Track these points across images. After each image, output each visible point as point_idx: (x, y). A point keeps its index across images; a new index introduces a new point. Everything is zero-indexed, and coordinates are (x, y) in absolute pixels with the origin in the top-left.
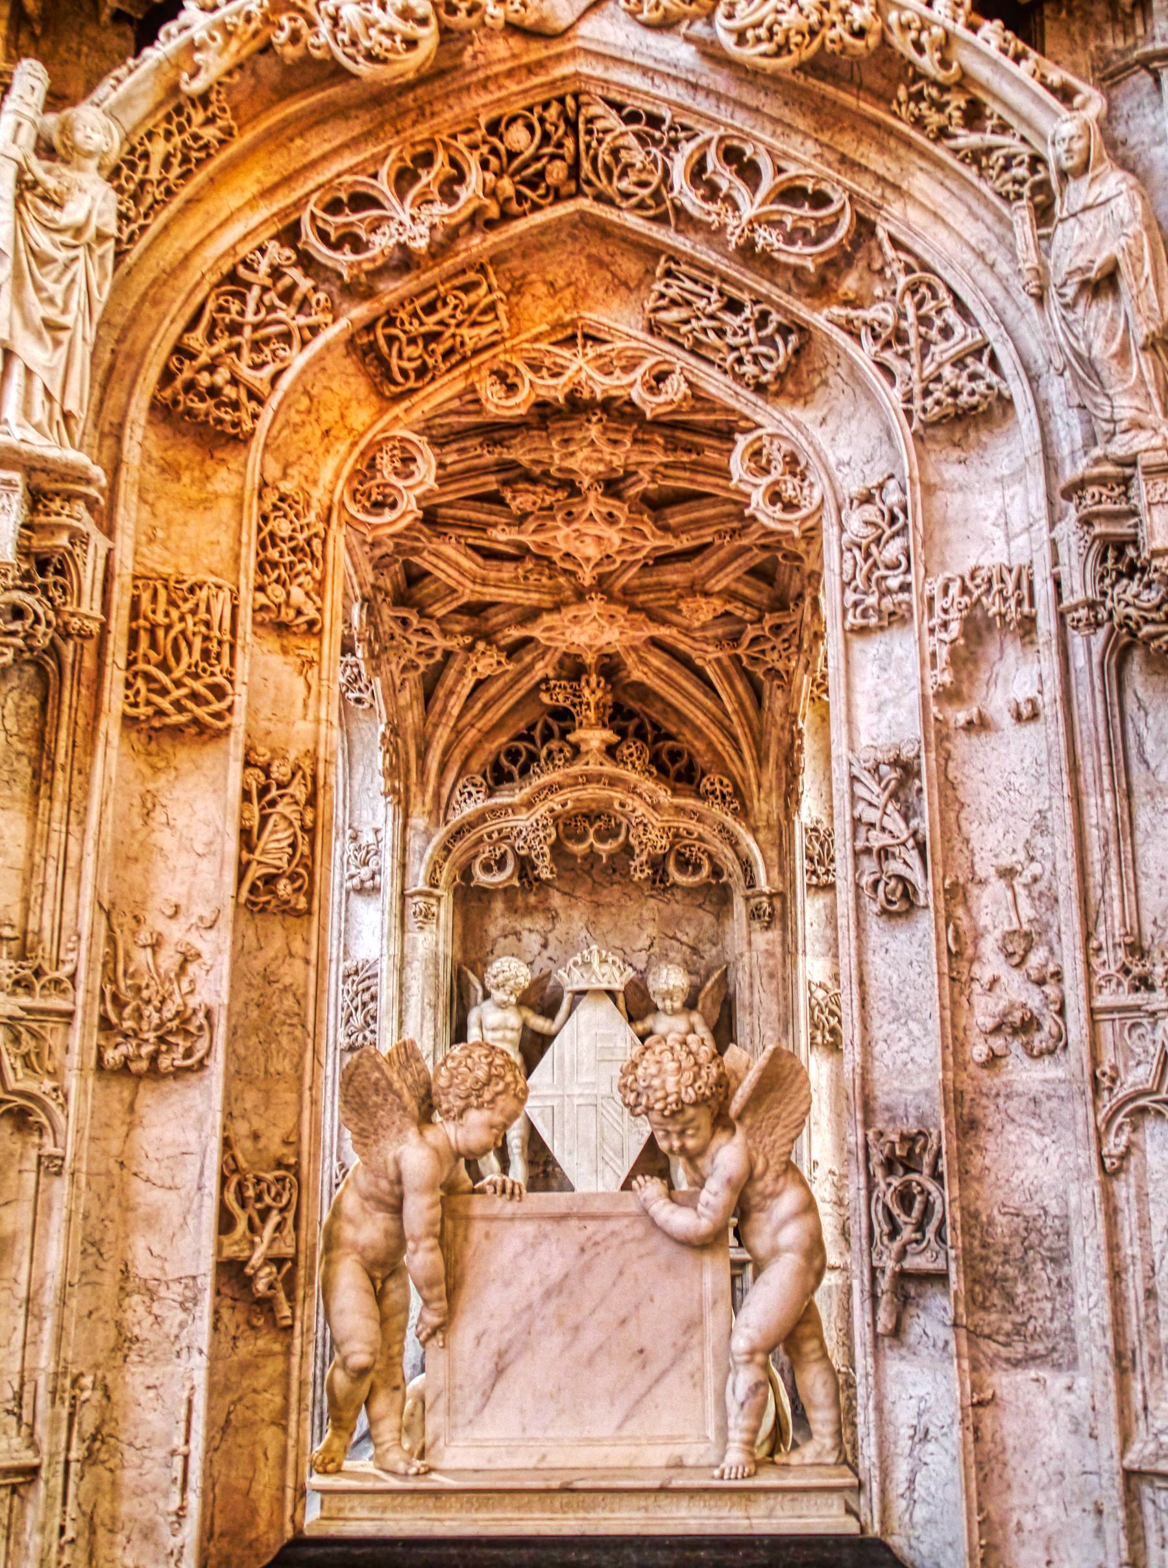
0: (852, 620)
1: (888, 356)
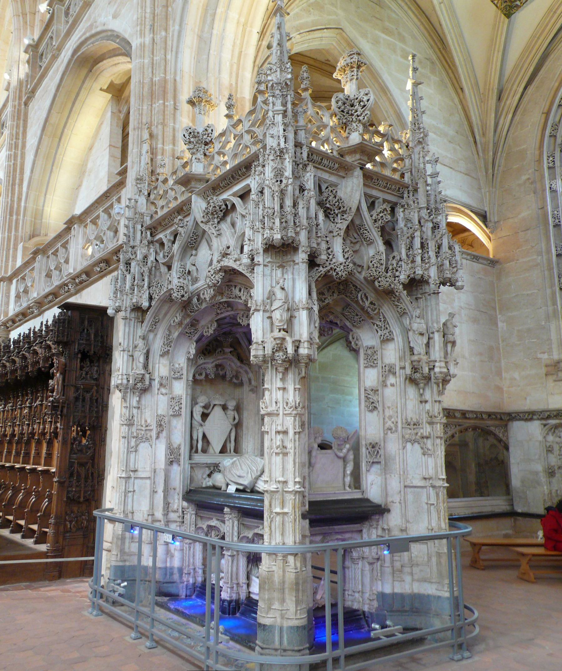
1: (378, 330)
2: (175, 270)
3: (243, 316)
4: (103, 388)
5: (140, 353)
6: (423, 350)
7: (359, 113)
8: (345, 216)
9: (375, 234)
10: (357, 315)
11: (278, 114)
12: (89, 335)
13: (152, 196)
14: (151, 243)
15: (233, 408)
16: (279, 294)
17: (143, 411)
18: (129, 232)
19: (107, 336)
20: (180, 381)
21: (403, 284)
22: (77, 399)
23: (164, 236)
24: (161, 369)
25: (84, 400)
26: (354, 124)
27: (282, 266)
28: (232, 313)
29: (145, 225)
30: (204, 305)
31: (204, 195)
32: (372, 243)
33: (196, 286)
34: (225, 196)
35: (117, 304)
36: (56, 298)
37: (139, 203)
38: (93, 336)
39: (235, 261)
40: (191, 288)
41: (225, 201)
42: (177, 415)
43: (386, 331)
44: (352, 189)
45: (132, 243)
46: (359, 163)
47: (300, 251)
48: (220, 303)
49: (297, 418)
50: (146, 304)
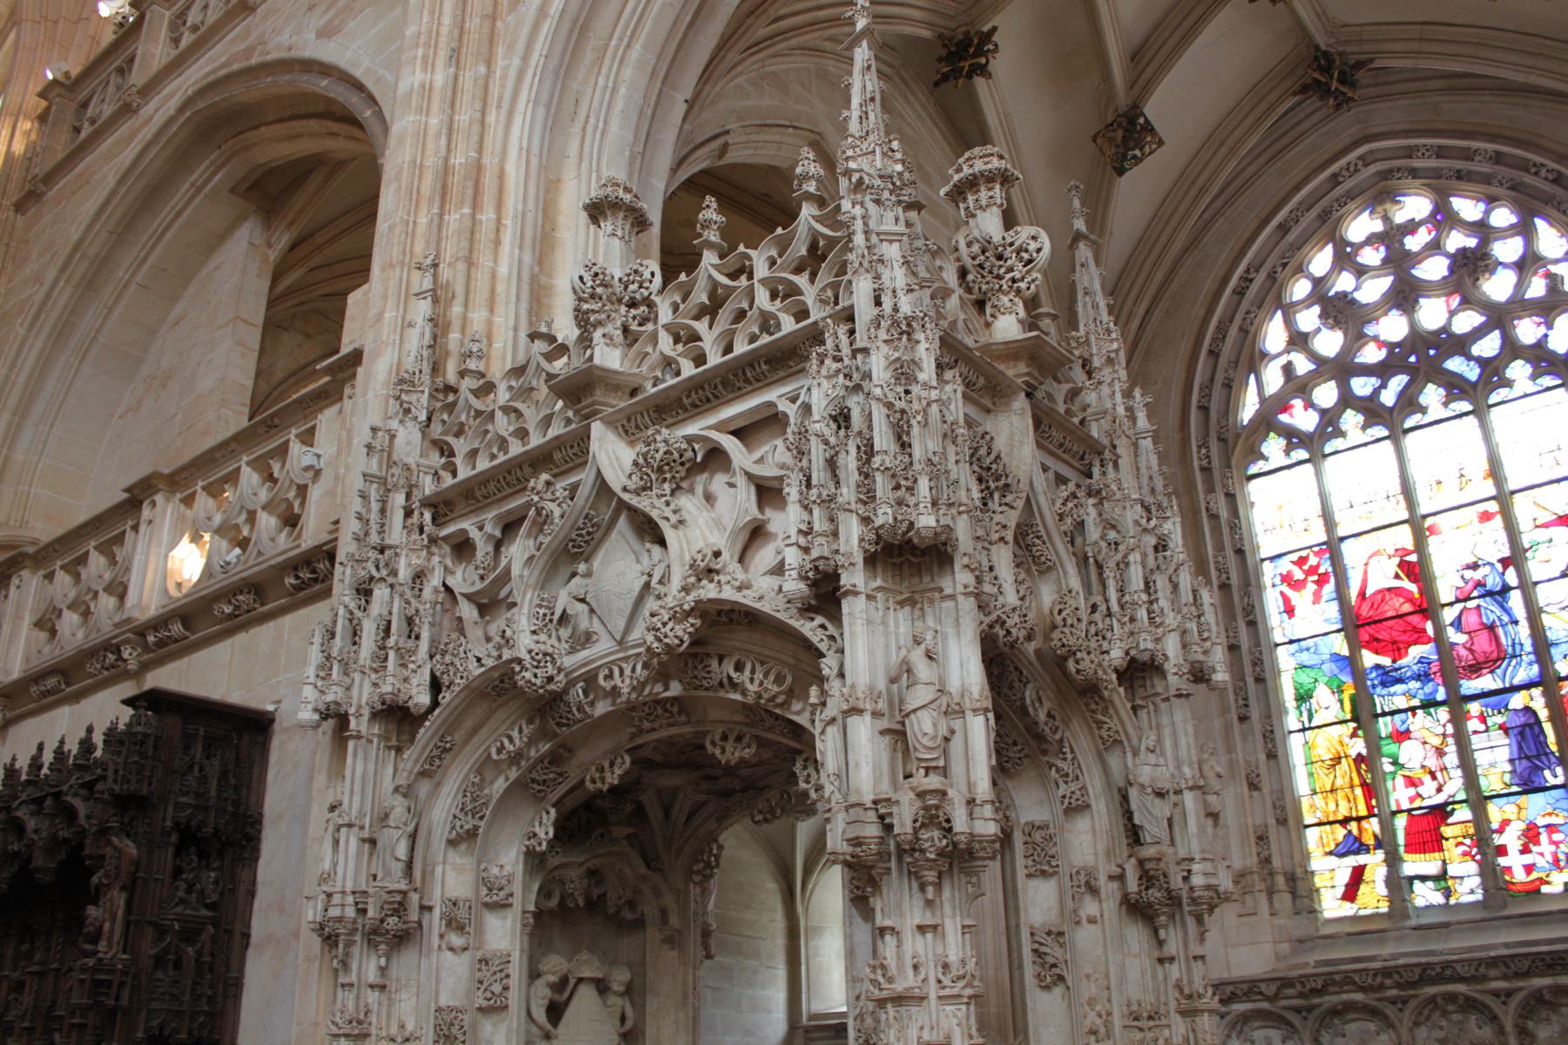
0: (1032, 870)
2: (525, 611)
3: (725, 738)
4: (230, 932)
5: (396, 833)
6: (1164, 835)
7: (1017, 275)
8: (1009, 499)
9: (1060, 547)
10: (1015, 744)
11: (891, 242)
12: (203, 780)
13: (436, 430)
14: (433, 540)
15: (622, 988)
16: (923, 670)
17: (396, 996)
18: (369, 511)
19: (249, 787)
20: (501, 913)
21: (1116, 671)
22: (159, 961)
23: (478, 527)
24: (453, 878)
25: (177, 965)
26: (1005, 299)
27: (911, 602)
28: (688, 729)
29: (417, 495)
30: (602, 708)
31: (628, 427)
32: (1050, 568)
33: (583, 655)
34: (692, 429)
35: (330, 698)
36: (68, 684)
37: (399, 441)
38: (214, 785)
39: (739, 589)
40: (568, 662)
41: (690, 440)
42: (494, 1008)
43: (1074, 786)
44: (1011, 438)
45: (374, 538)
46: (1026, 383)
47: (957, 567)
48: (658, 702)
49: (972, 1008)
50: (424, 699)
